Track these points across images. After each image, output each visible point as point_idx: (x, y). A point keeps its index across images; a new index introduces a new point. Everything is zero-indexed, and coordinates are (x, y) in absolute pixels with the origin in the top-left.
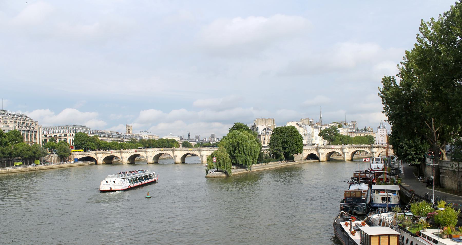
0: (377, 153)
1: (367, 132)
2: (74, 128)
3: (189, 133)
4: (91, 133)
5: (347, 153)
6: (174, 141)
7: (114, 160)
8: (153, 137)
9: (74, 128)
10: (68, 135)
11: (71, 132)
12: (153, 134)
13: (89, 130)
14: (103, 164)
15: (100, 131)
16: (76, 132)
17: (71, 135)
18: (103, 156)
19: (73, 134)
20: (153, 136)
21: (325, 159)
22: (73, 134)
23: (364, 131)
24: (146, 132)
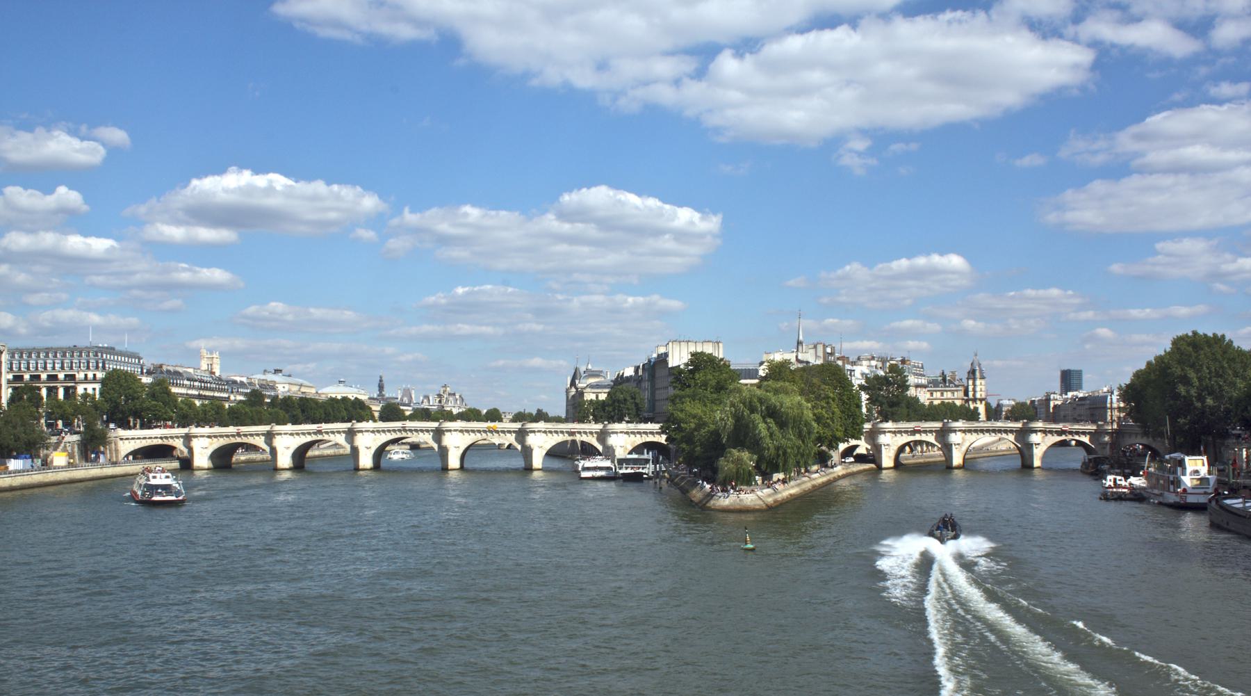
0: (1040, 447)
1: (949, 387)
2: (100, 354)
3: (381, 381)
4: (145, 371)
5: (957, 446)
6: (358, 404)
7: (240, 457)
8: (300, 388)
9: (100, 354)
10: (80, 376)
11: (88, 368)
12: (300, 381)
13: (139, 362)
14: (208, 469)
15: (169, 368)
16: (104, 367)
17: (90, 375)
18: (211, 444)
19: (95, 375)
20: (301, 385)
21: (891, 464)
22: (95, 375)
23: (941, 383)
24: (280, 374)
